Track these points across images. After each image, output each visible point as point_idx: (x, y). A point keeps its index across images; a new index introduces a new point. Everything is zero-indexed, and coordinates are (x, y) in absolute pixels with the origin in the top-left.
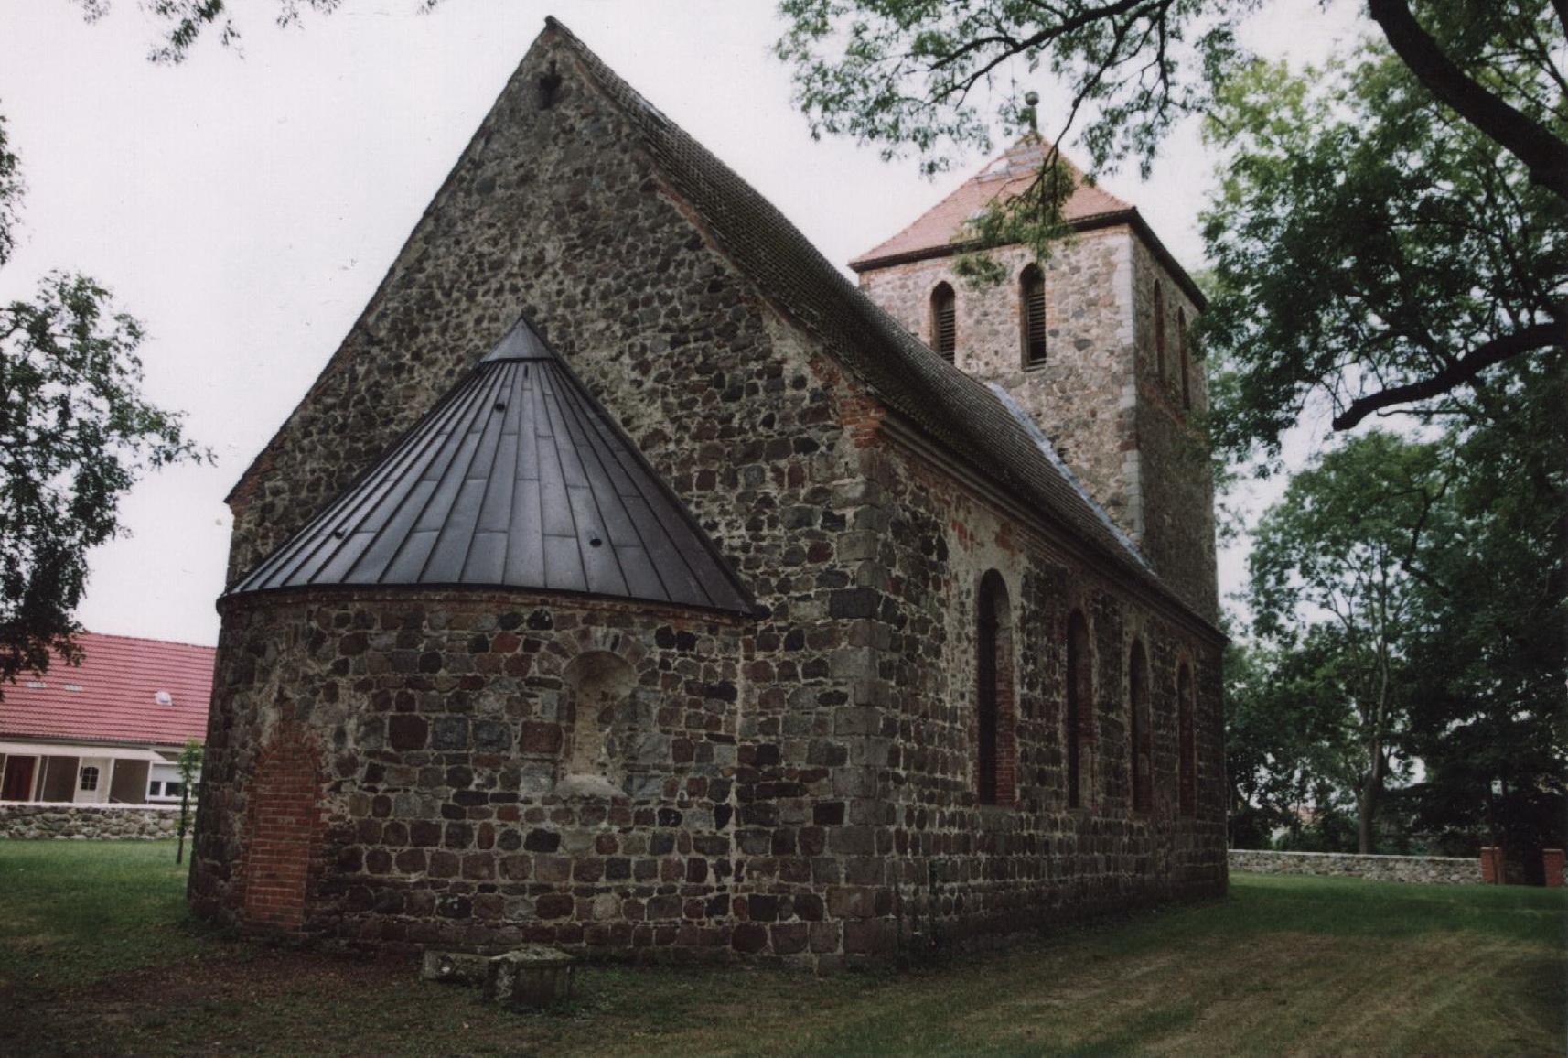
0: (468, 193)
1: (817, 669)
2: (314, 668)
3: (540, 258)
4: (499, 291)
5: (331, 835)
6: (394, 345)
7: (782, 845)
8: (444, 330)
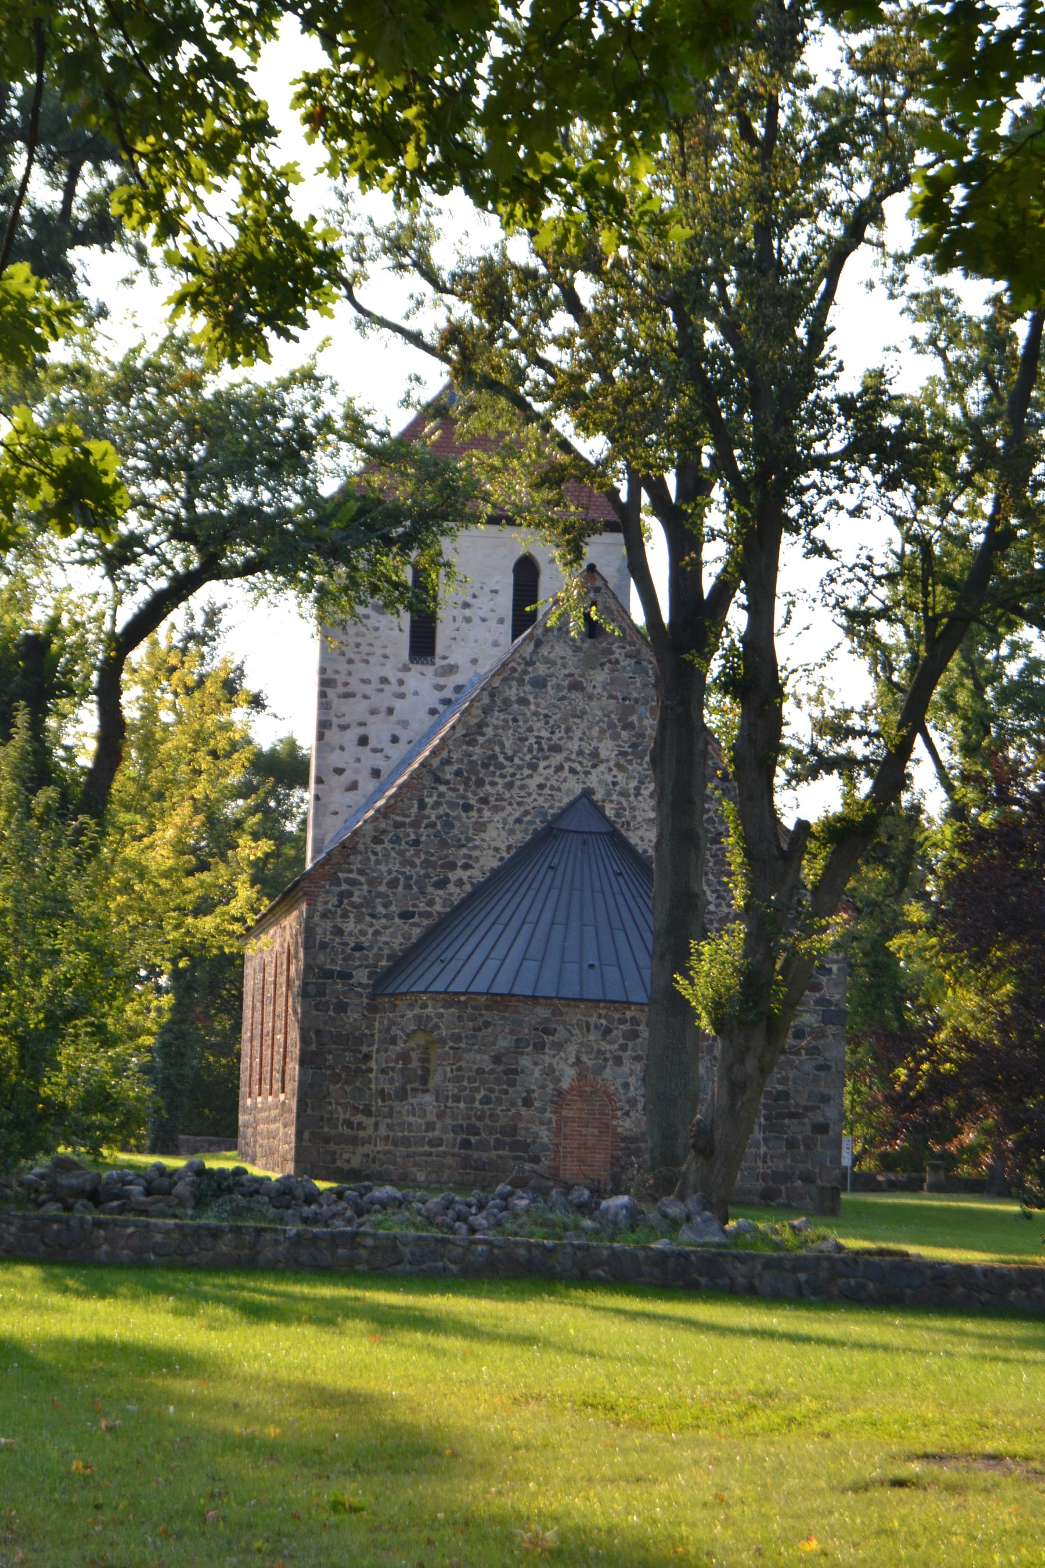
0: (521, 682)
1: (813, 1051)
2: (605, 1046)
3: (595, 754)
4: (560, 768)
5: (625, 1139)
6: (461, 788)
7: (792, 1144)
8: (510, 786)
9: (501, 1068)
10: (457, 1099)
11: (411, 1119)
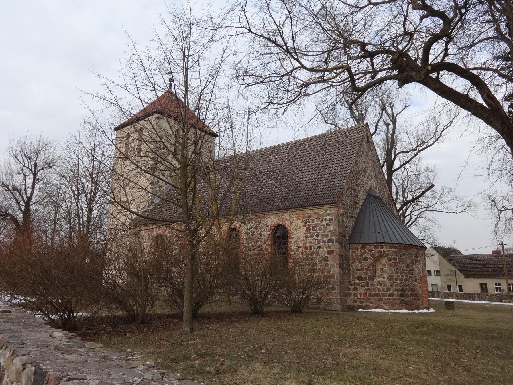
9: (409, 269)
10: (397, 280)
11: (379, 287)
